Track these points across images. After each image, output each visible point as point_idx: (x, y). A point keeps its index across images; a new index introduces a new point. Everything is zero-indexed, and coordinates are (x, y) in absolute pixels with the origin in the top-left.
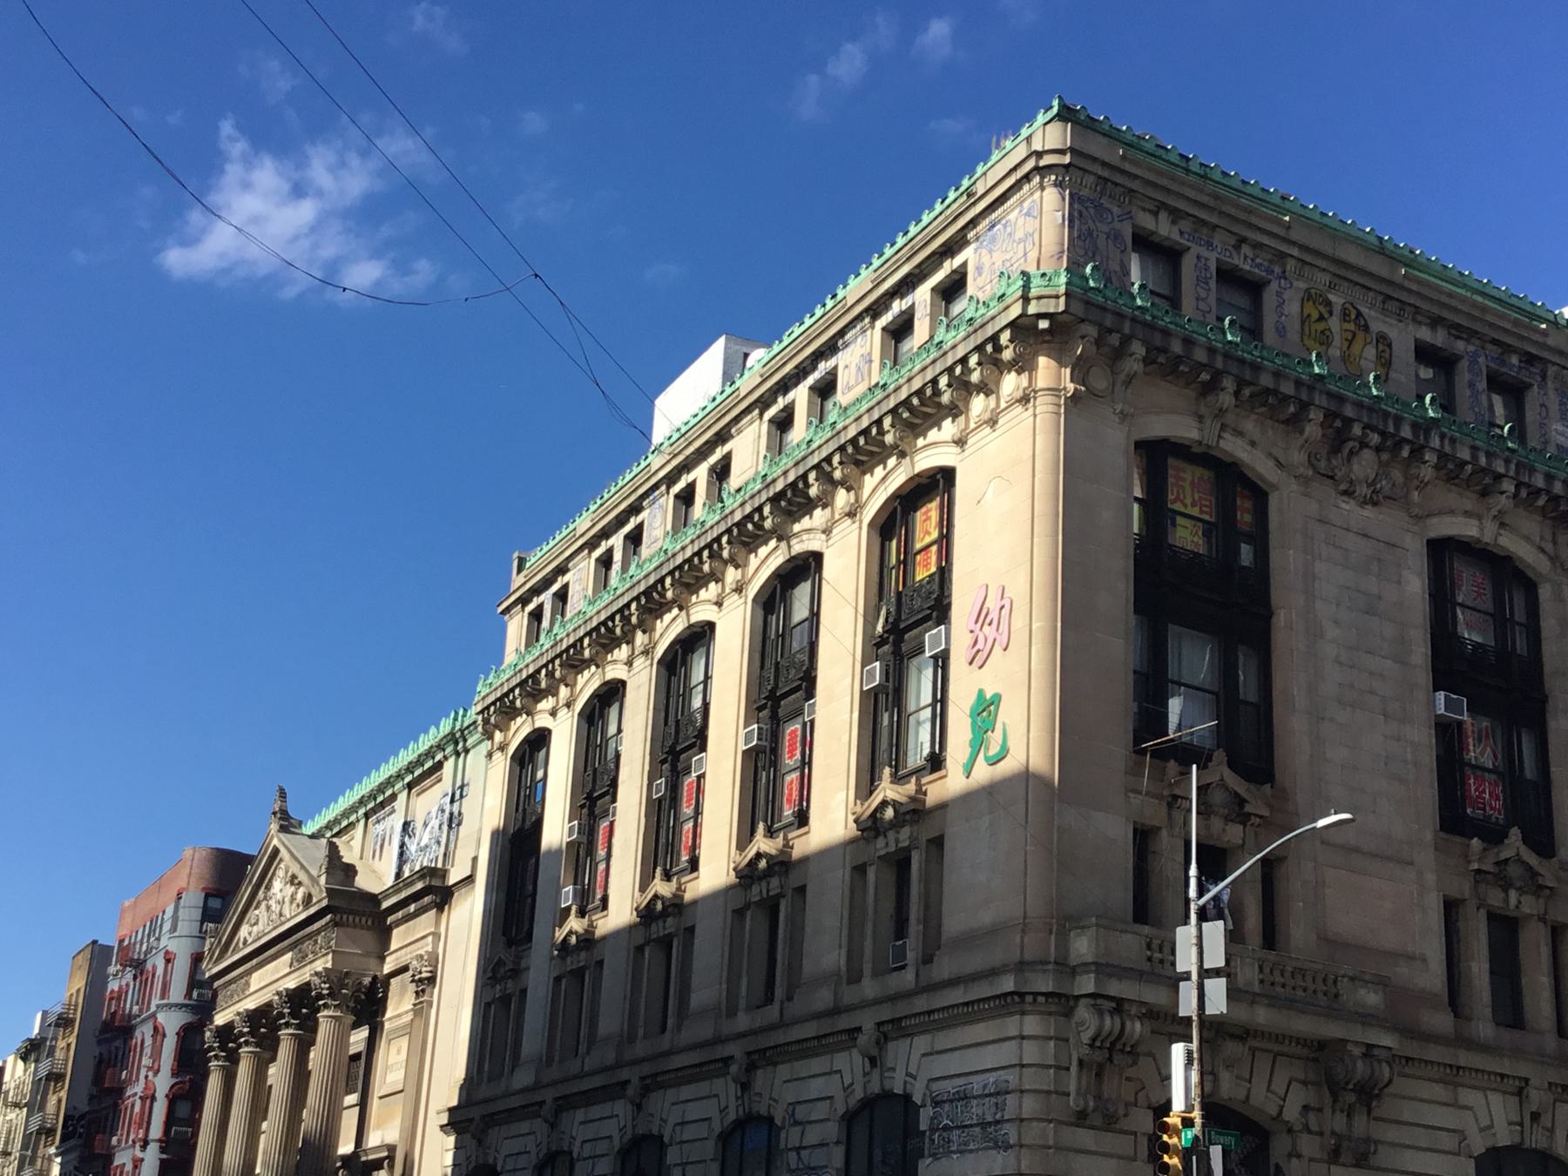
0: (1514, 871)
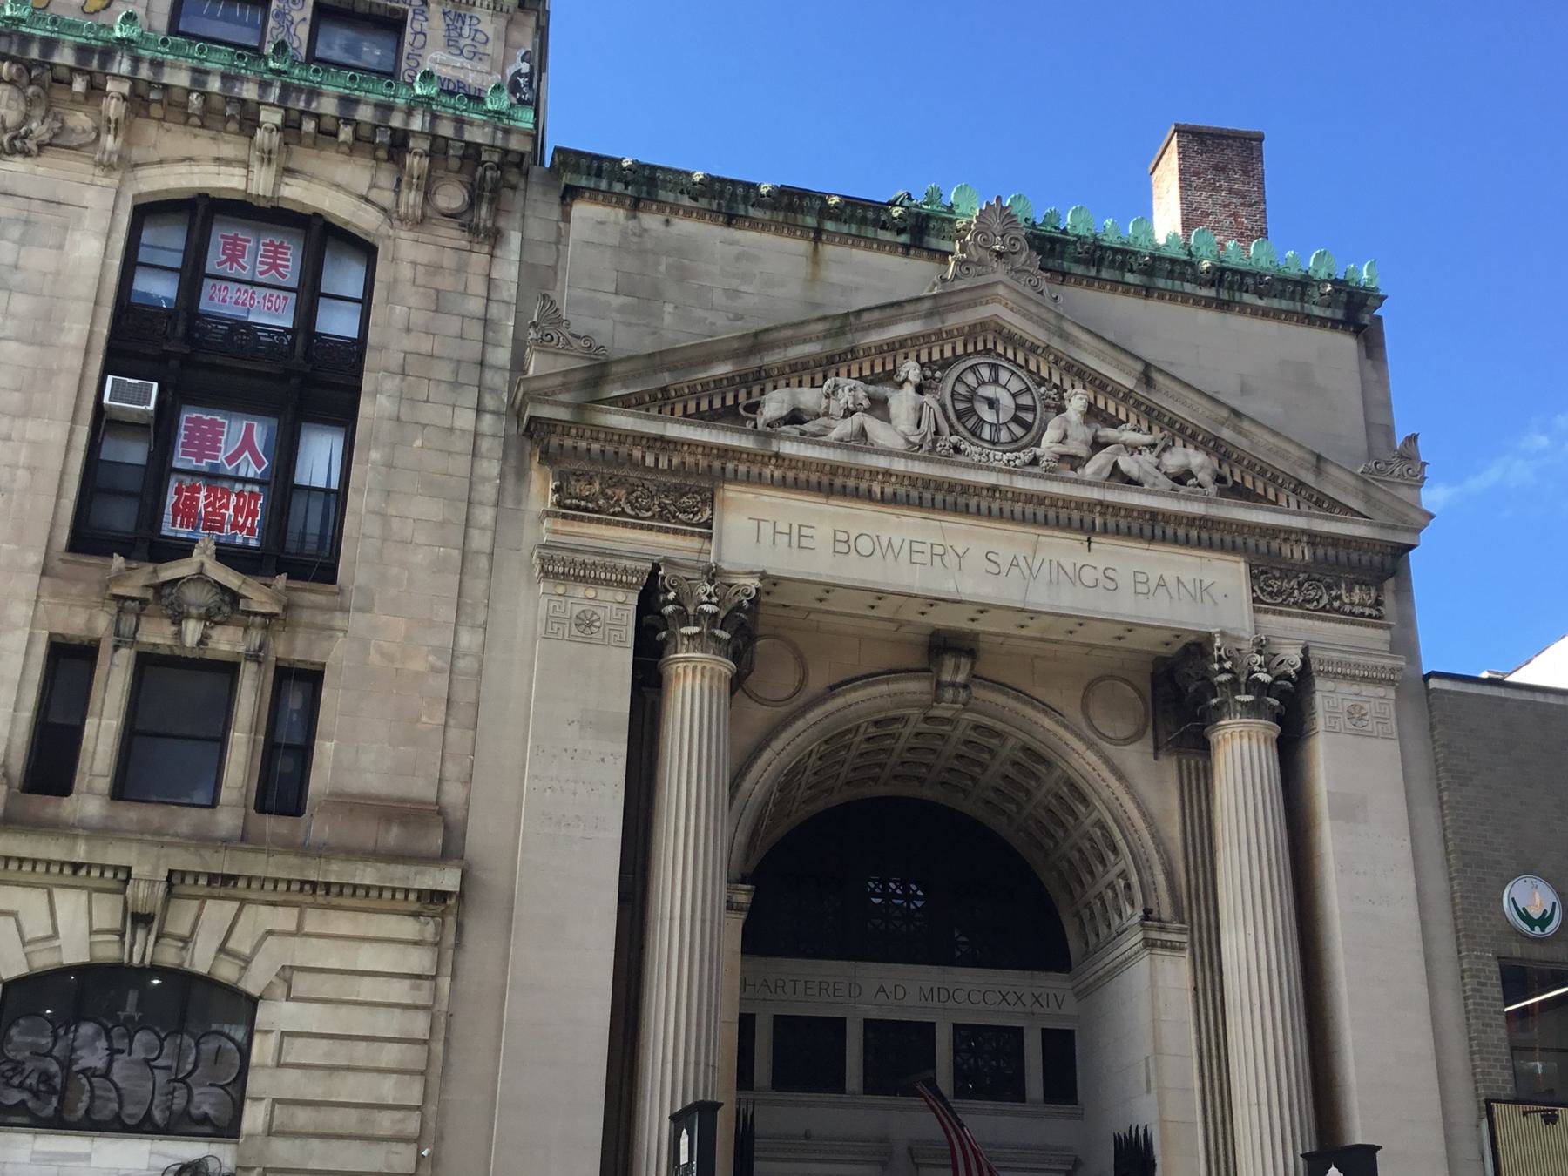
0: (196, 596)
